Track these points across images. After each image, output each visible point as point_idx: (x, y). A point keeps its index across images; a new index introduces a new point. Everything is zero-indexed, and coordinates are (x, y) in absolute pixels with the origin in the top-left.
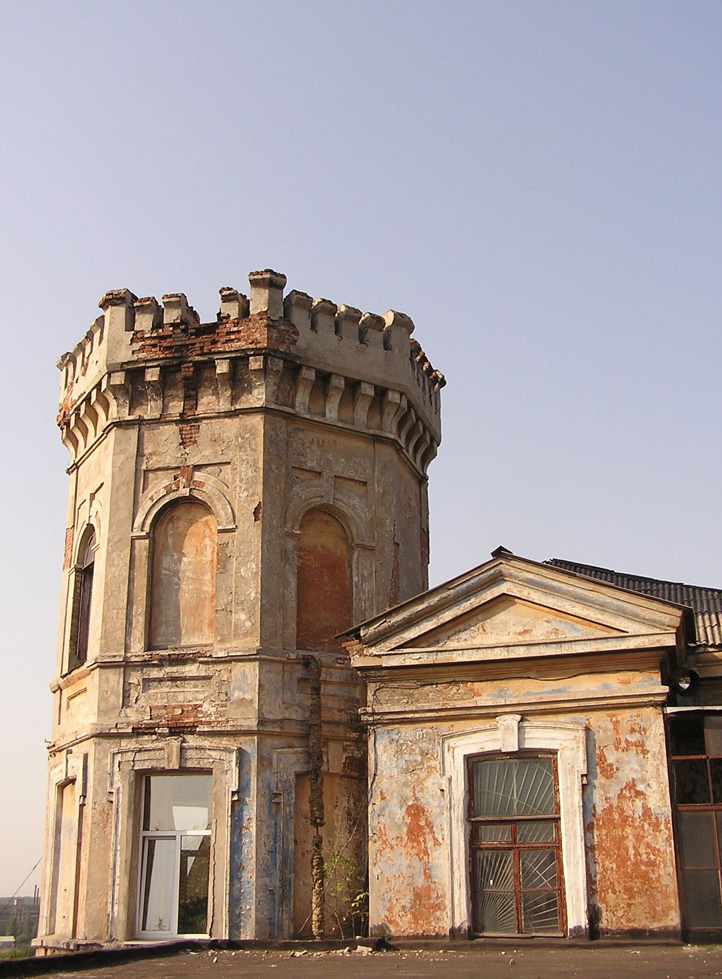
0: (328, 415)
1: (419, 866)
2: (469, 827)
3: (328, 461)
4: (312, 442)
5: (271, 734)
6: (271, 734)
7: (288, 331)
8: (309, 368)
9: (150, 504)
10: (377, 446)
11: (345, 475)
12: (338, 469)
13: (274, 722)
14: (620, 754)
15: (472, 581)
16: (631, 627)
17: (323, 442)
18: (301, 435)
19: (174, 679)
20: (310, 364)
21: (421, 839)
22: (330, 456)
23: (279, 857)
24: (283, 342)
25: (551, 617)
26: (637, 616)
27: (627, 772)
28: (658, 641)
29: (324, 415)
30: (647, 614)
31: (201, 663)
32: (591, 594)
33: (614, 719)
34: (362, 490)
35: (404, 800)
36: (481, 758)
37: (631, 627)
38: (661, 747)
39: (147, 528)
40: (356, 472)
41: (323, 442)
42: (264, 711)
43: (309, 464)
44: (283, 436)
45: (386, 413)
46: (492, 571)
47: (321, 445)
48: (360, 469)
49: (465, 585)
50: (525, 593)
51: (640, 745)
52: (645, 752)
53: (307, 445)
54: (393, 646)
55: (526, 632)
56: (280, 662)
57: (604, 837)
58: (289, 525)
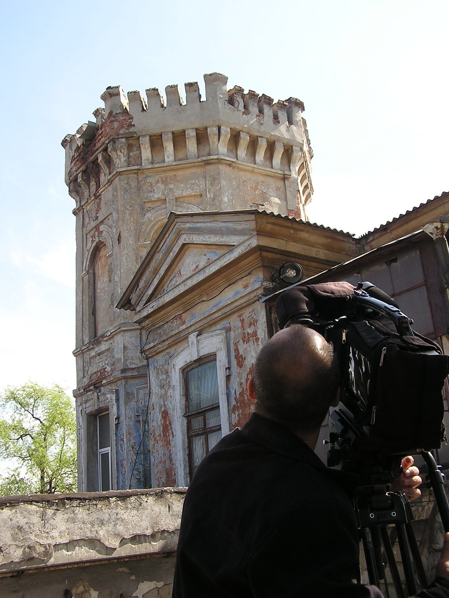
0: (167, 160)
1: (167, 452)
2: (185, 421)
3: (171, 190)
4: (157, 182)
5: (133, 377)
6: (133, 377)
7: (125, 119)
8: (145, 136)
9: (87, 253)
10: (208, 167)
11: (184, 194)
12: (177, 194)
13: (133, 369)
14: (246, 346)
15: (167, 242)
16: (233, 240)
17: (166, 179)
18: (149, 180)
19: (99, 354)
20: (144, 133)
21: (168, 434)
22: (171, 186)
23: (142, 456)
24: (123, 127)
25: (206, 251)
26: (236, 230)
27: (249, 359)
28: (249, 245)
29: (164, 161)
30: (239, 227)
31: (106, 341)
32: (213, 225)
33: (242, 318)
34: (199, 200)
35: (161, 408)
36: (188, 369)
37: (233, 240)
38: (265, 334)
39: (87, 269)
40: (193, 190)
41: (166, 179)
42: (128, 363)
43: (156, 196)
44: (134, 184)
45: (211, 142)
46: (174, 230)
47: (163, 182)
48: (196, 187)
49: (164, 247)
50: (197, 239)
51: (255, 333)
52: (257, 339)
53: (154, 185)
54: (144, 302)
55: (197, 267)
56: (137, 329)
57: (241, 415)
58: (142, 240)
